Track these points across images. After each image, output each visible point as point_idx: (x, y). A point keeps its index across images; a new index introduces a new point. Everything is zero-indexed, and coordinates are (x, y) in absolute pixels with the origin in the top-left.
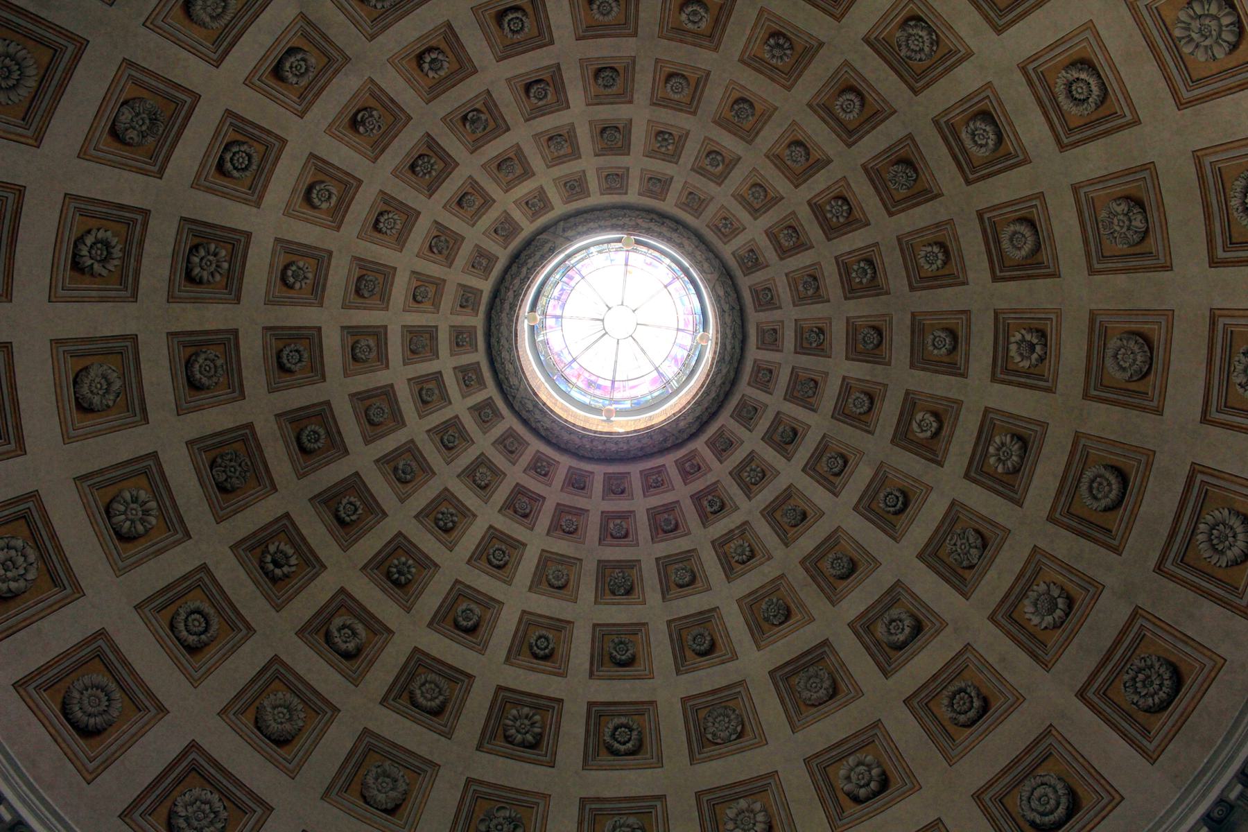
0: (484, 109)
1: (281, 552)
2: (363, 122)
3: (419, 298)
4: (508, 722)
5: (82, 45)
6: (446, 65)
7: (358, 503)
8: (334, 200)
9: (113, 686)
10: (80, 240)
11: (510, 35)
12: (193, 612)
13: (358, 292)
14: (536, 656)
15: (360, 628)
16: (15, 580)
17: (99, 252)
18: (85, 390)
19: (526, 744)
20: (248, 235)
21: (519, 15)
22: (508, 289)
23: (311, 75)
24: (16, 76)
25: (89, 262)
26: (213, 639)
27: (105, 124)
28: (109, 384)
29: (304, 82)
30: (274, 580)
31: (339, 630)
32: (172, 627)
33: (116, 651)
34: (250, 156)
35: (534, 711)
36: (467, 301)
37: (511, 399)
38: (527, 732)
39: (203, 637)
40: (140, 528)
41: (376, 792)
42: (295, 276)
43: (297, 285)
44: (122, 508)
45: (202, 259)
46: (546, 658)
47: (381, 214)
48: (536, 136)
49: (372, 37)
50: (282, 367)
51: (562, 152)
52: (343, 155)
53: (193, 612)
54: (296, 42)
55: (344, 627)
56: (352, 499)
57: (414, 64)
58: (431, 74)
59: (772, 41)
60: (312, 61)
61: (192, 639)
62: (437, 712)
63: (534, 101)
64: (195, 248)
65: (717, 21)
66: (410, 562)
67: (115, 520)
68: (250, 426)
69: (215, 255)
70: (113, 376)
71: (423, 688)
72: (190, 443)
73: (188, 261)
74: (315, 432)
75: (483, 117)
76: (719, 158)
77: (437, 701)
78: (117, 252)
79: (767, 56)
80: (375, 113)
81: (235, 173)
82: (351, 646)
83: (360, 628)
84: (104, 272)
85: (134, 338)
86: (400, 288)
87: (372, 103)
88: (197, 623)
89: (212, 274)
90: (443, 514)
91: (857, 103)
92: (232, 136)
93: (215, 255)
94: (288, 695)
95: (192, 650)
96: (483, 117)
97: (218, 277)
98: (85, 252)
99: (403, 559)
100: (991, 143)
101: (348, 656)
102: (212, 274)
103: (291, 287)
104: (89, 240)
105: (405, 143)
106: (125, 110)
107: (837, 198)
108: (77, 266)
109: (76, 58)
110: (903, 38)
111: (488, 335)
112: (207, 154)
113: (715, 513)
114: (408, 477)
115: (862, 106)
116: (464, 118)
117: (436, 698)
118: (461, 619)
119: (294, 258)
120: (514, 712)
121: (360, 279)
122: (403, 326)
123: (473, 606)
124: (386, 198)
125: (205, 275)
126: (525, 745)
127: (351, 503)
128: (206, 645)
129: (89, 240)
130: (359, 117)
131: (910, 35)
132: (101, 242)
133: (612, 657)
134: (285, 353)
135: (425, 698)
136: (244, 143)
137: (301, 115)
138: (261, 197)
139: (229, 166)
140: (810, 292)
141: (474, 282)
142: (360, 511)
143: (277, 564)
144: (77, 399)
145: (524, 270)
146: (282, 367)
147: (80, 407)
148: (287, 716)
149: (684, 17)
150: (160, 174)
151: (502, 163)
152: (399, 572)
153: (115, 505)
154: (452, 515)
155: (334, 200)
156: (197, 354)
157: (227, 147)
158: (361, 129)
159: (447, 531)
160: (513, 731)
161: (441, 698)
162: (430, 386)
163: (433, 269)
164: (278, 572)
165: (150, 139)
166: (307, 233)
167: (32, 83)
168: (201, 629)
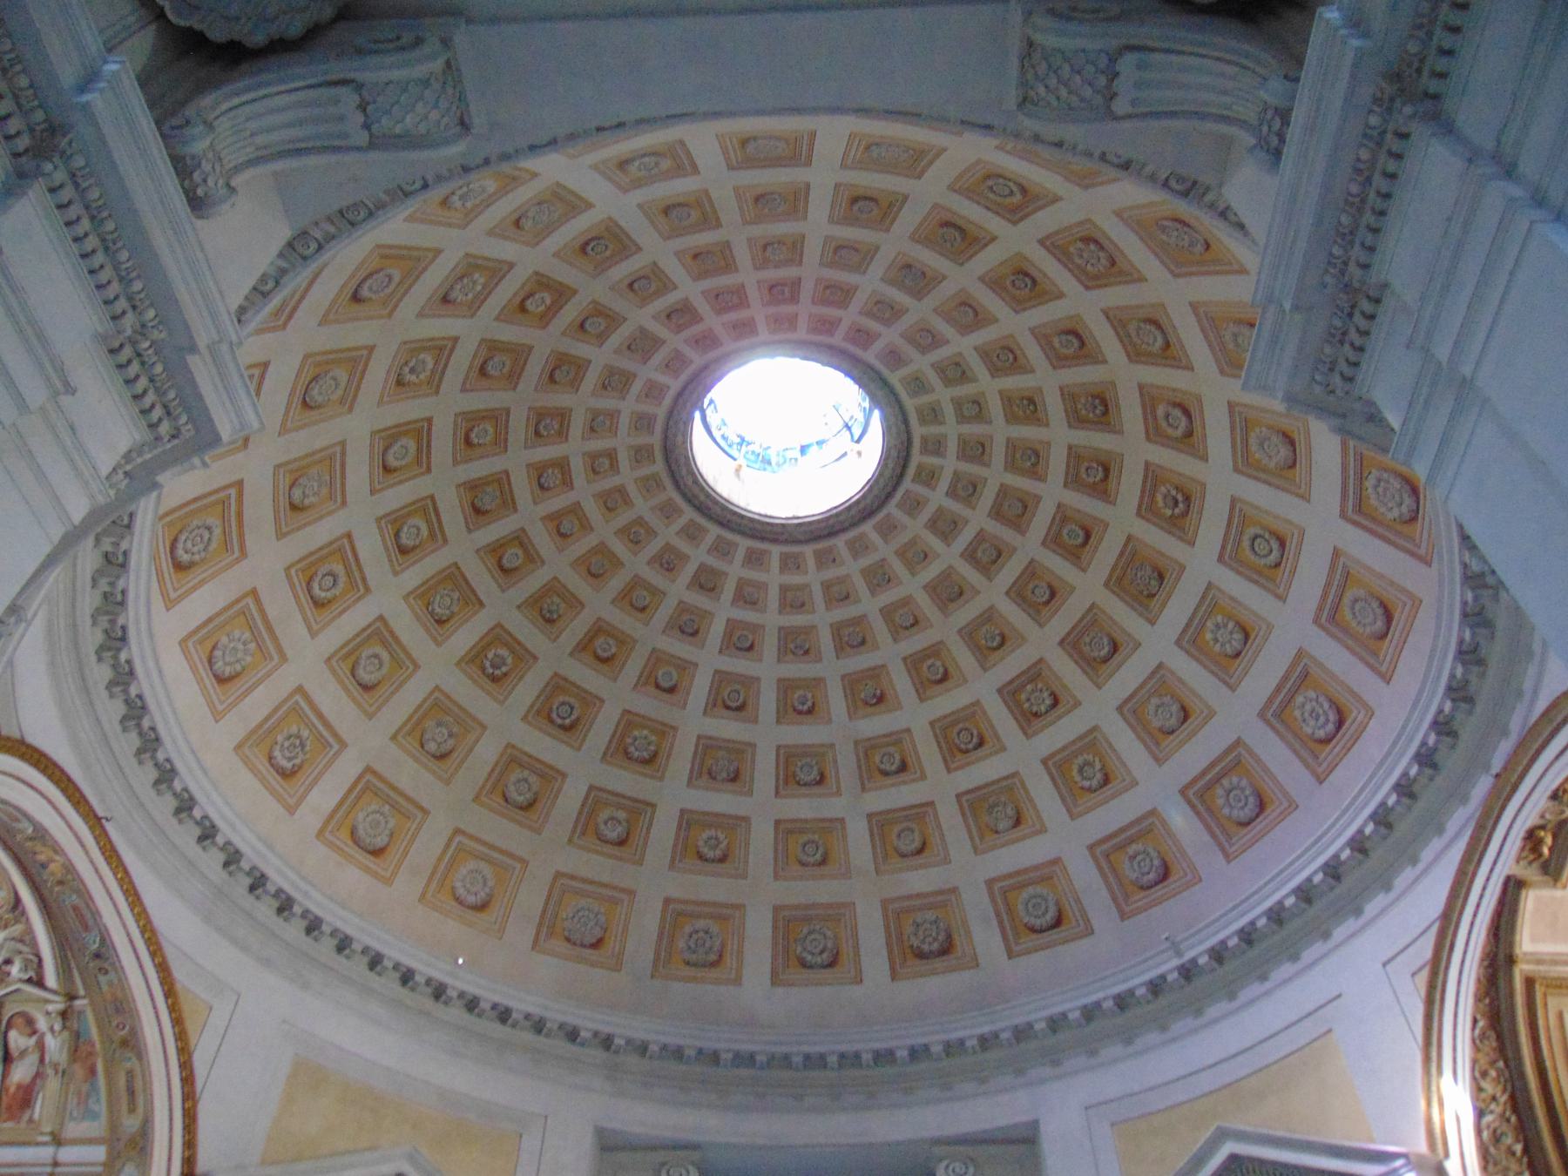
2: (874, 695)
3: (922, 555)
5: (990, 883)
6: (796, 696)
7: (1083, 470)
8: (930, 662)
10: (1090, 790)
16: (1322, 706)
17: (1088, 771)
18: (1173, 722)
20: (1000, 691)
22: (852, 517)
23: (884, 750)
24: (1034, 901)
26: (1264, 528)
27: (1017, 833)
29: (891, 749)
32: (1278, 565)
34: (959, 734)
40: (1231, 625)
42: (993, 639)
44: (1228, 646)
48: (763, 611)
49: (832, 746)
51: (750, 589)
52: (902, 683)
56: (1084, 476)
60: (877, 759)
63: (751, 637)
64: (1036, 715)
65: (591, 640)
67: (1239, 648)
69: (1028, 700)
70: (1151, 708)
73: (1047, 712)
78: (1080, 760)
81: (975, 733)
84: (1097, 759)
86: (931, 572)
87: (859, 703)
88: (1261, 546)
92: (959, 756)
93: (1028, 700)
97: (1040, 686)
98: (1095, 783)
100: (405, 529)
105: (860, 662)
107: (548, 489)
108: (1106, 780)
113: (782, 285)
116: (807, 652)
121: (952, 601)
125: (1046, 694)
127: (1088, 475)
129: (1086, 784)
133: (963, 239)
137: (908, 730)
138: (973, 704)
139: (975, 740)
140: (601, 418)
141: (875, 537)
143: (1176, 503)
144: (1183, 723)
145: (831, 522)
146: (1053, 594)
147: (1186, 718)
149: (614, 650)
150: (1015, 775)
151: (800, 606)
154: (1018, 406)
156: (1095, 659)
157: (967, 751)
158: (878, 692)
163: (898, 567)
166: (963, 657)
167: (1030, 890)
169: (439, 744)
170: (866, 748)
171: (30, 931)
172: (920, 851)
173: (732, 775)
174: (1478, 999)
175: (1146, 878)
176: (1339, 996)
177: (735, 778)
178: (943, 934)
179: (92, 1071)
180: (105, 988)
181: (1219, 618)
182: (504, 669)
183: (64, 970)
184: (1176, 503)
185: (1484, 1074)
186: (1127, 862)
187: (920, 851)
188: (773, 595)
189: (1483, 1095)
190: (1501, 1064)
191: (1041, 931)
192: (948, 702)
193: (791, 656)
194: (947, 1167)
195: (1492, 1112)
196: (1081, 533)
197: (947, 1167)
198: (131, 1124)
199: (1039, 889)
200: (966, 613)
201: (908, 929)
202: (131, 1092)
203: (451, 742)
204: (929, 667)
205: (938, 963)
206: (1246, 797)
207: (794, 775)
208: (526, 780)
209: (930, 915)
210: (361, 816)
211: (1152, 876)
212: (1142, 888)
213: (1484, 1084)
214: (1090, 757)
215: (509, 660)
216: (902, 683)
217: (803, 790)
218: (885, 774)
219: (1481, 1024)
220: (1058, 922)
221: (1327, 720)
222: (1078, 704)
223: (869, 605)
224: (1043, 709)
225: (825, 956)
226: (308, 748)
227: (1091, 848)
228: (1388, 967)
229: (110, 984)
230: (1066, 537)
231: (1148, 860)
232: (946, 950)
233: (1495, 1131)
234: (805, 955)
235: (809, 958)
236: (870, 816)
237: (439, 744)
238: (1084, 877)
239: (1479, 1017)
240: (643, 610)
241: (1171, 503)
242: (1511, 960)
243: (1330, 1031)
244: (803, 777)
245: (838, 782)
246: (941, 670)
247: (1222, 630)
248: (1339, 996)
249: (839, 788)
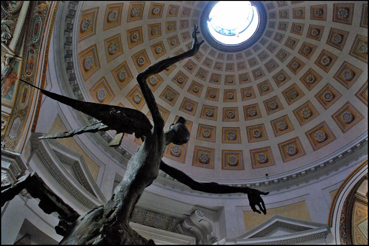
0: (199, 75)
1: (309, 79)
3: (243, 67)
4: (342, 17)
5: (223, 151)
6: (195, 87)
7: (294, 64)
8: (230, 93)
9: (343, 113)
10: (256, 137)
11: (183, 79)
12: (326, 97)
13: (247, 80)
14: (322, 13)
15: (324, 58)
18: (283, 128)
19: (348, 12)
21: (179, 80)
25: (259, 134)
26: (331, 92)
27: (234, 141)
28: (281, 124)
29: (211, 110)
30: (315, 80)
31: (325, 63)
32: (329, 101)
33: (335, 113)
35: (338, 11)
36: (239, 56)
37: (258, 38)
38: (345, 12)
39: (331, 94)
40: (309, 111)
41: (366, 50)
43: (250, 93)
44: (305, 116)
45: (251, 114)
46: (322, 11)
47: (229, 83)
49: (197, 103)
50: (268, 89)
52: (221, 96)
53: (326, 97)
54: (205, 115)
55: (324, 62)
56: (293, 65)
57: (198, 92)
58: (198, 88)
59: (154, 34)
60: (207, 111)
61: (332, 97)
62: (342, 36)
66: (305, 49)
67: (308, 117)
68: (282, 92)
69: (250, 112)
70: (279, 124)
71: (336, 40)
72: (289, 105)
73: (253, 116)
74: (280, 78)
75: (201, 74)
76: (183, 24)
77: (339, 36)
78: (256, 130)
79: (157, 32)
80: (210, 94)
81: (233, 114)
82: (328, 59)
83: (324, 58)
84: (260, 131)
85: (271, 122)
87: (209, 96)
88: (328, 96)
89: (254, 111)
90: (291, 44)
91: (155, 10)
92: (227, 118)
93: (250, 112)
94: (342, 74)
95: (334, 96)
96: (201, 74)
97: (254, 109)
98: (257, 136)
99: (304, 50)
101: (331, 60)
102: (254, 111)
103: (251, 94)
104: (255, 136)
105: (214, 85)
106: (230, 139)
108: (261, 136)
109: (225, 150)
110: (137, 14)
111: (245, 49)
112: (232, 121)
114: (284, 54)
115: (154, 9)
117: (338, 37)
118: (316, 34)
119: (245, 95)
120: (339, 16)
121: (244, 81)
122: (251, 67)
123: (312, 31)
124: (225, 83)
126: (348, 13)
127: (294, 65)
128: (332, 94)
129: (255, 136)
130: (213, 97)
131: (135, 14)
132: (255, 133)
134: (265, 90)
135: (339, 39)
136: (227, 115)
139: (232, 116)
142: (295, 63)
143: (312, 80)
146: (268, 89)
147: (287, 129)
148: (348, 73)
149: (160, 51)
152: (308, 50)
153: (305, 117)
155: (230, 93)
158: (215, 95)
159: (295, 42)
160: (345, 16)
161: (338, 36)
162: (261, 56)
164: (314, 79)
165: (233, 132)
166: (239, 95)
168: (329, 95)
169: (112, 50)
170: (205, 107)
171: (15, 25)
172: (209, 137)
173: (171, 99)
175: (262, 161)
177: (171, 100)
178: (208, 158)
179: (13, 83)
180: (30, 57)
181: (307, 109)
182: (135, 40)
183: (18, 45)
184: (312, 80)
185: (343, 213)
186: (258, 156)
187: (209, 137)
188: (204, 59)
191: (231, 166)
192: (230, 105)
193: (199, 76)
194: (198, 212)
196: (283, 78)
197: (198, 212)
198: (22, 106)
199: (234, 156)
200: (245, 85)
201: (199, 155)
202: (25, 96)
203: (114, 51)
204: (230, 94)
205: (205, 165)
206: (294, 150)
207: (186, 106)
208: (124, 73)
209: (206, 153)
210: (88, 57)
211: (263, 161)
212: (260, 163)
214: (259, 130)
215: (137, 39)
216: (221, 96)
217: (186, 111)
218: (207, 115)
220: (236, 165)
221: (323, 138)
222: (261, 117)
223: (224, 73)
224: (252, 115)
225: (177, 154)
226: (89, 28)
227: (250, 150)
229: (32, 57)
230: (279, 78)
231: (263, 157)
232: (207, 163)
234: (172, 152)
235: (173, 153)
236: (199, 124)
237: (112, 50)
238: (247, 155)
240: (172, 45)
241: (310, 80)
244: (187, 107)
245: (195, 112)
246: (232, 97)
247: (306, 112)
249: (195, 114)
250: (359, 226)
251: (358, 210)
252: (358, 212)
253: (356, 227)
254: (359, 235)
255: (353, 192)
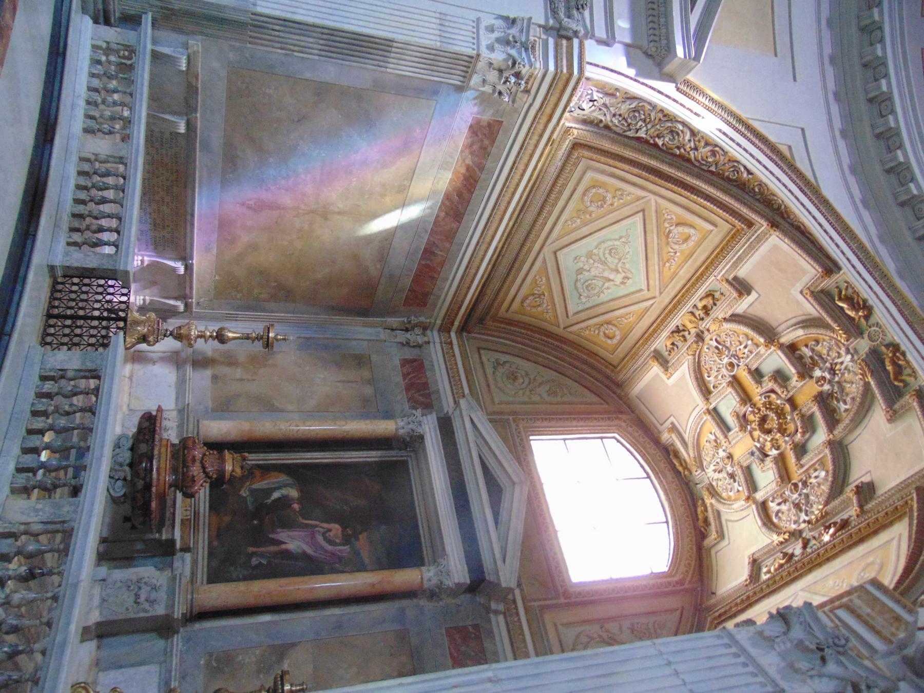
174: (761, 184)
176: (795, 80)
185: (714, 153)
189: (702, 144)
190: (713, 169)
195: (690, 141)
213: (709, 148)
219: (745, 175)
228: (800, 130)
233: (678, 134)
239: (750, 176)
242: (774, 225)
243: (776, 55)
248: (795, 80)
250: (638, 218)
251: (692, 231)
252: (687, 230)
253: (639, 205)
254: (612, 205)
255: (778, 219)
